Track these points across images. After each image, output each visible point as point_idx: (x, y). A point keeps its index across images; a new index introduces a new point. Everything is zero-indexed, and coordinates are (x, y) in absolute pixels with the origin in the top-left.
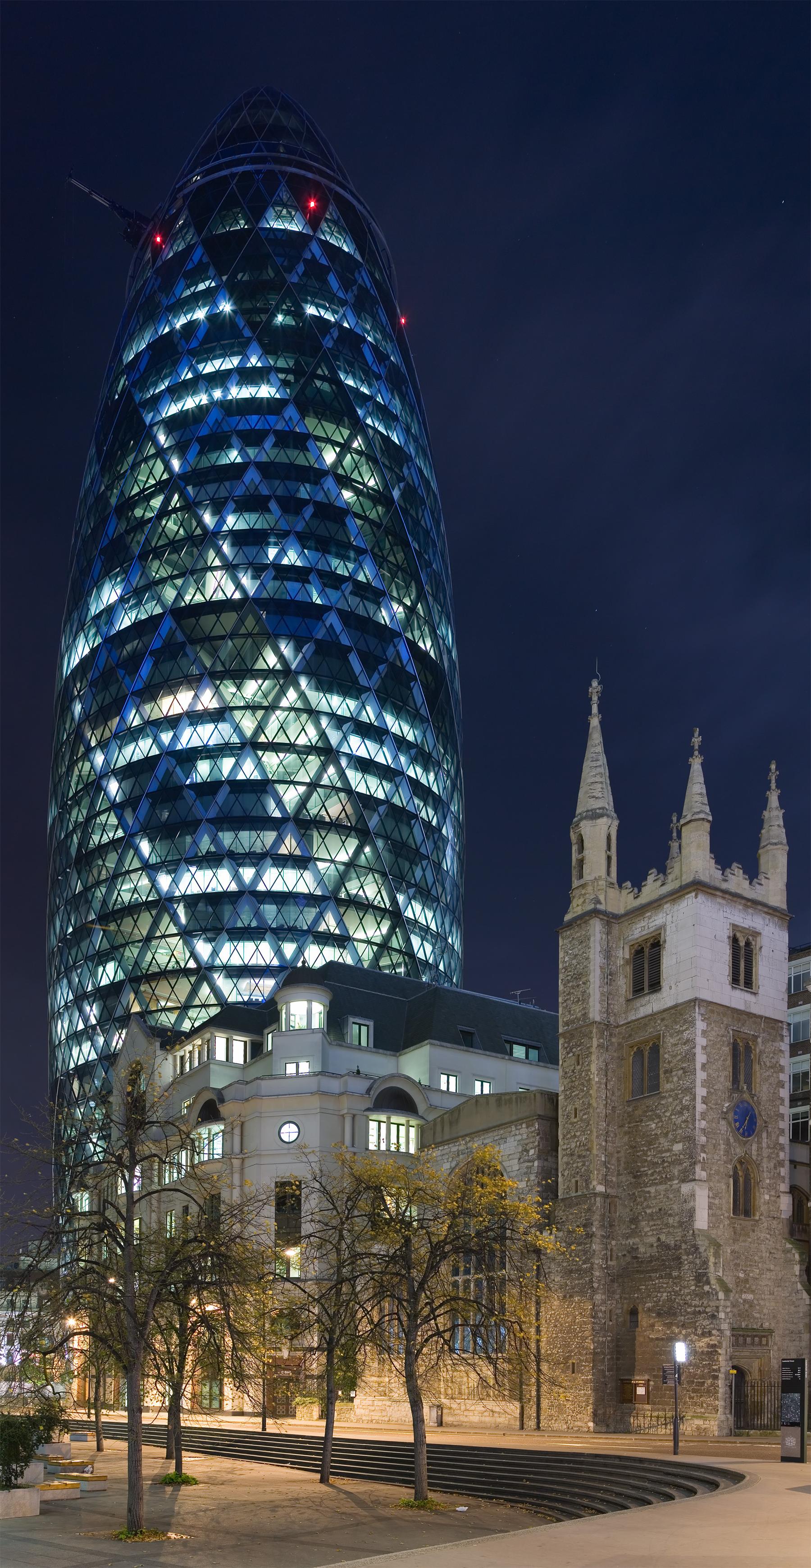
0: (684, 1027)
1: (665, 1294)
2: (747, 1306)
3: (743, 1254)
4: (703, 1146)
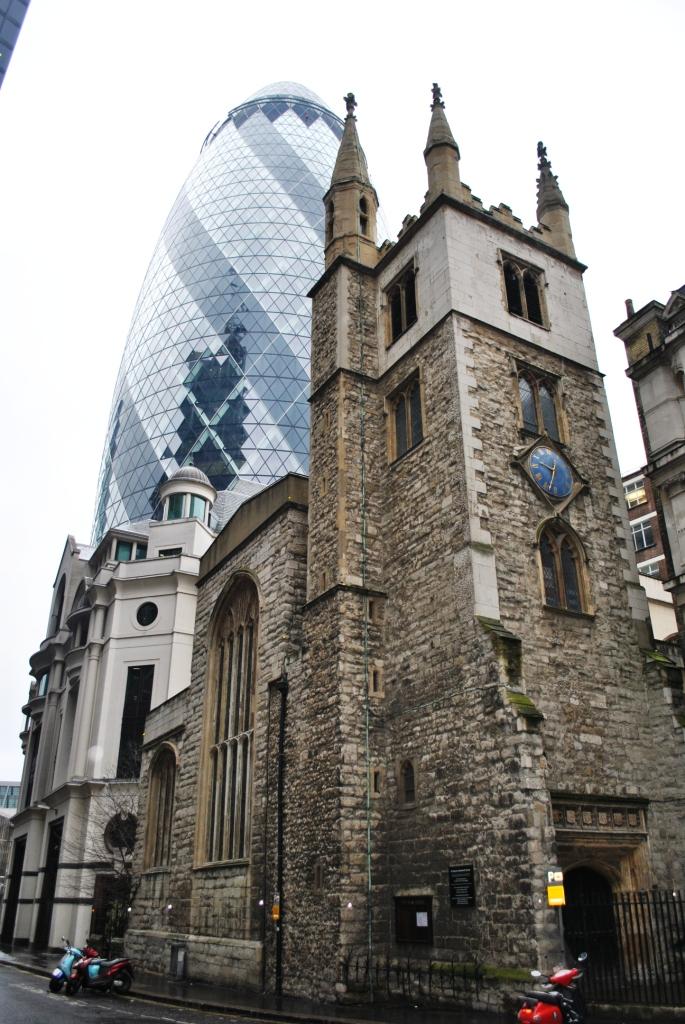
0: (444, 348)
1: (445, 735)
2: (591, 756)
3: (574, 667)
4: (480, 495)
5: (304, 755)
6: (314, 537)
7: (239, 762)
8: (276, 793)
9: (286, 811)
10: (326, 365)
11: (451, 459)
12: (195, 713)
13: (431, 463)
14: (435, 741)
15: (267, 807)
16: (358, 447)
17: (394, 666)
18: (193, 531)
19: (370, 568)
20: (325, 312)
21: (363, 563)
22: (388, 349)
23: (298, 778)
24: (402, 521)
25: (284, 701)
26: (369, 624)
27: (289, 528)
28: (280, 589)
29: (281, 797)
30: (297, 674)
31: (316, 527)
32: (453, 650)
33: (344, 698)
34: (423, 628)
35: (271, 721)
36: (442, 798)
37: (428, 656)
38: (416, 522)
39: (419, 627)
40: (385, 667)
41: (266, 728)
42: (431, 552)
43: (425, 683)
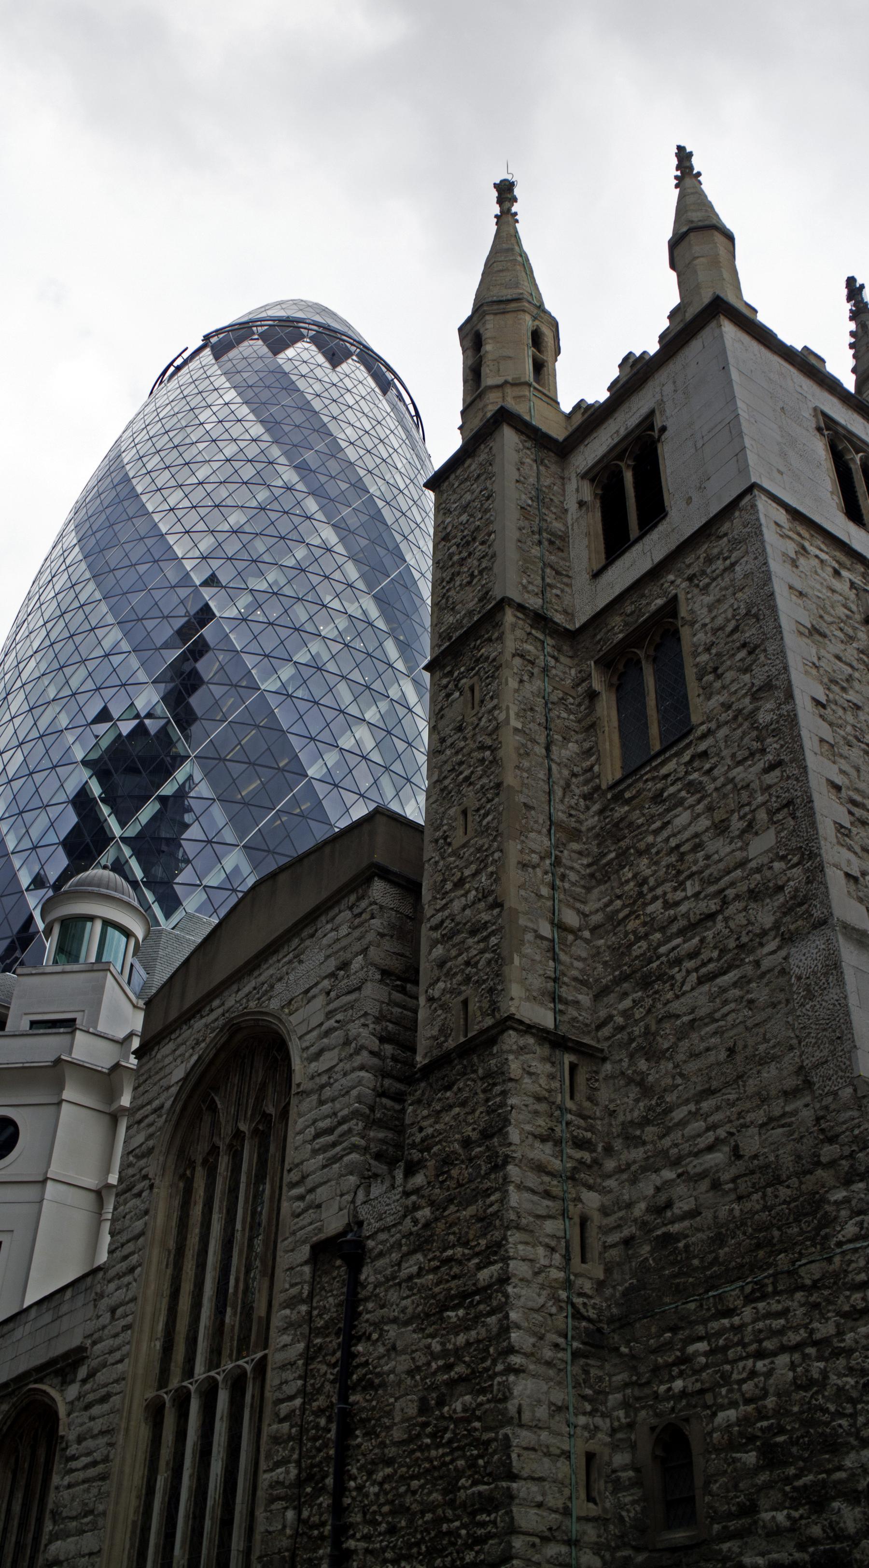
1: (783, 1360)
5: (408, 1406)
6: (435, 928)
7: (220, 1428)
8: (325, 1500)
9: (352, 1544)
10: (468, 601)
11: (770, 757)
12: (113, 1318)
13: (716, 772)
14: (753, 1374)
15: (296, 1535)
16: (540, 750)
17: (629, 1205)
18: (100, 989)
19: (564, 992)
20: (465, 508)
21: (555, 980)
22: (596, 575)
23: (389, 1462)
24: (641, 895)
25: (354, 1284)
26: (570, 1112)
27: (373, 917)
28: (347, 1043)
29: (338, 1510)
30: (390, 1221)
31: (444, 908)
32: (799, 1157)
33: (517, 1268)
34: (708, 1115)
35: (315, 1332)
36: (781, 1516)
37: (726, 1176)
38: (680, 895)
39: (694, 1115)
40: (605, 1211)
41: (301, 1346)
42: (723, 952)
43: (719, 1240)
